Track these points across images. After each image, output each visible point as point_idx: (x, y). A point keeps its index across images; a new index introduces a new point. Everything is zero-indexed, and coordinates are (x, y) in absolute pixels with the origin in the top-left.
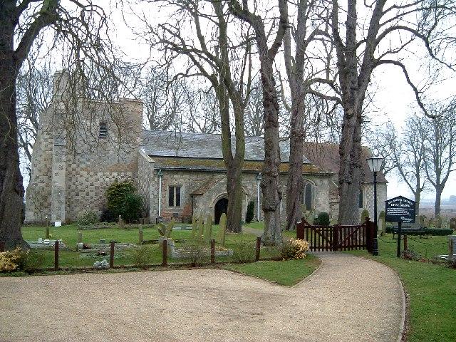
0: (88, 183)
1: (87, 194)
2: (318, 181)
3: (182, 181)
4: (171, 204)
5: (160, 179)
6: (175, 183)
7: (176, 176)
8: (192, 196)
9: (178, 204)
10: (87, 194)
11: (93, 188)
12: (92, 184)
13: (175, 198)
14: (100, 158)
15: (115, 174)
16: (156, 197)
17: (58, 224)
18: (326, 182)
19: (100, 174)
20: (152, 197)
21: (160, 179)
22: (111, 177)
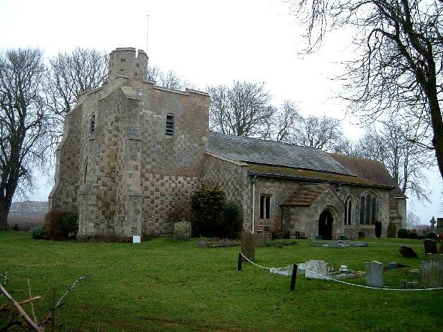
0: (153, 189)
1: (153, 202)
2: (381, 193)
3: (275, 191)
4: (262, 217)
5: (254, 186)
6: (267, 192)
7: (268, 184)
8: (281, 206)
9: (268, 217)
10: (153, 202)
11: (158, 194)
12: (157, 190)
13: (265, 209)
14: (166, 158)
15: (181, 179)
16: (250, 207)
17: (137, 239)
18: (387, 195)
19: (166, 178)
20: (245, 207)
21: (254, 186)
22: (177, 182)
